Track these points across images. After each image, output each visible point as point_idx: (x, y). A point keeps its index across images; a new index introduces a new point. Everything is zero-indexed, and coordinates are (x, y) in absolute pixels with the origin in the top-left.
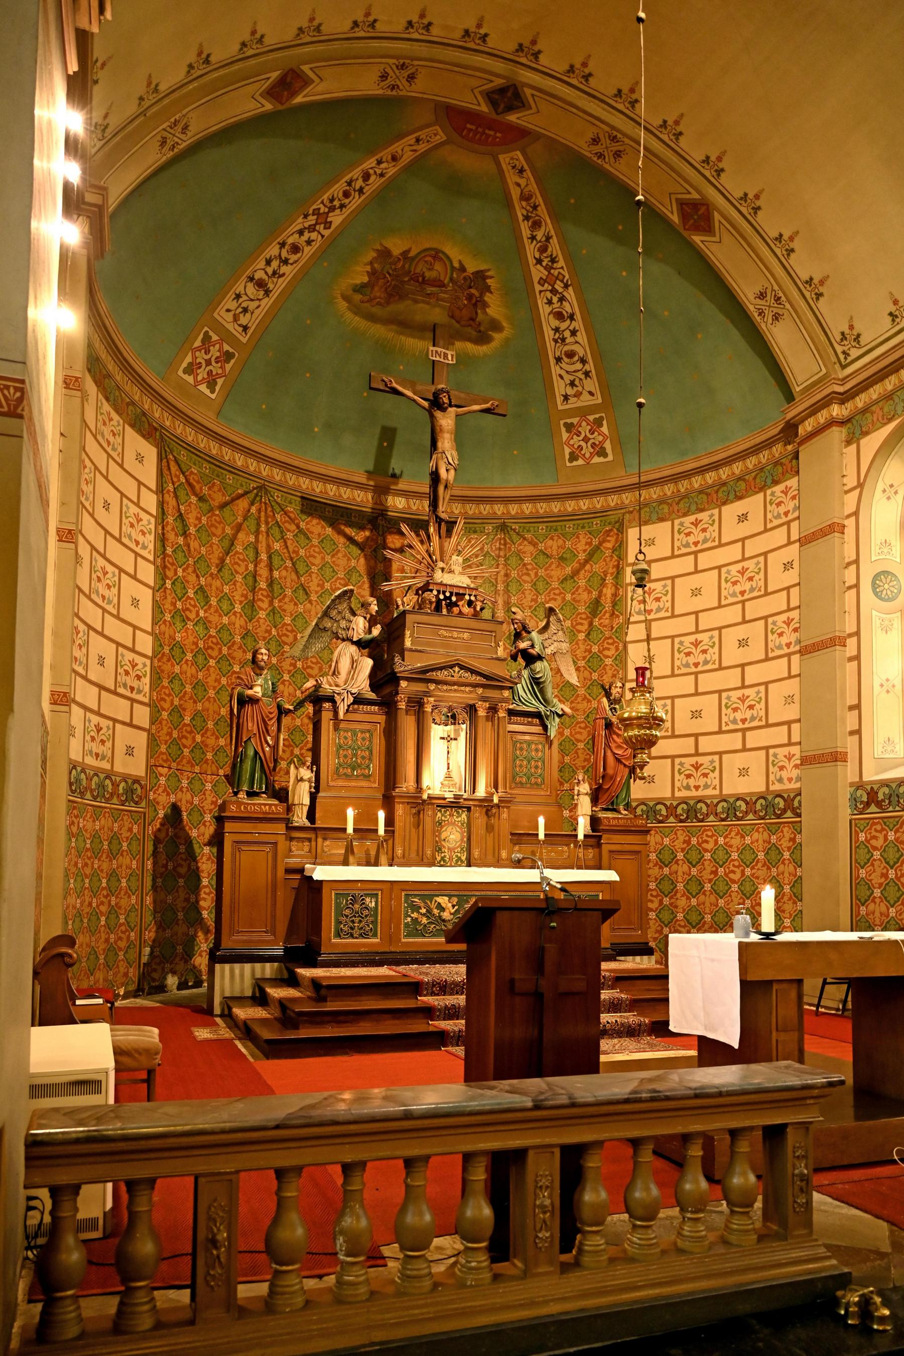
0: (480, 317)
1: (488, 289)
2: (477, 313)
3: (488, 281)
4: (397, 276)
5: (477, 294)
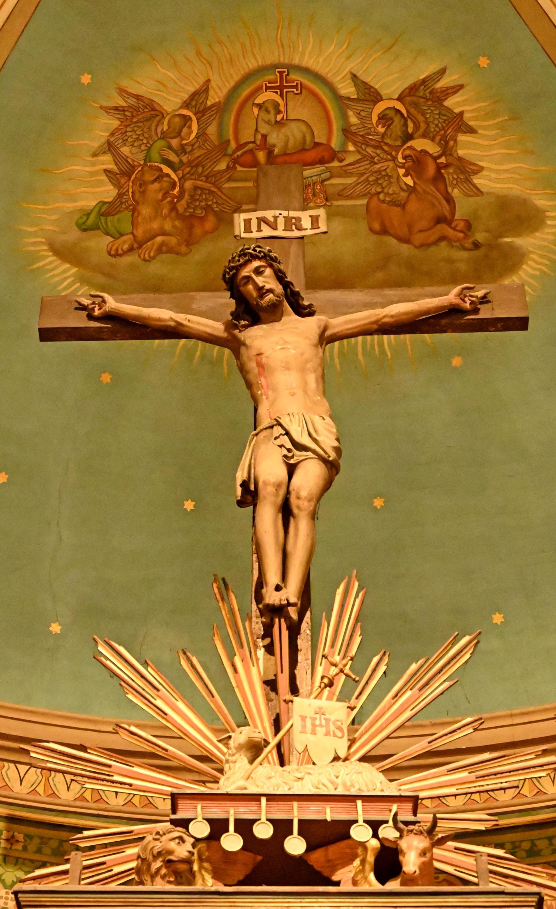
0: (464, 206)
1: (459, 123)
2: (449, 200)
3: (448, 103)
4: (194, 165)
5: (433, 148)
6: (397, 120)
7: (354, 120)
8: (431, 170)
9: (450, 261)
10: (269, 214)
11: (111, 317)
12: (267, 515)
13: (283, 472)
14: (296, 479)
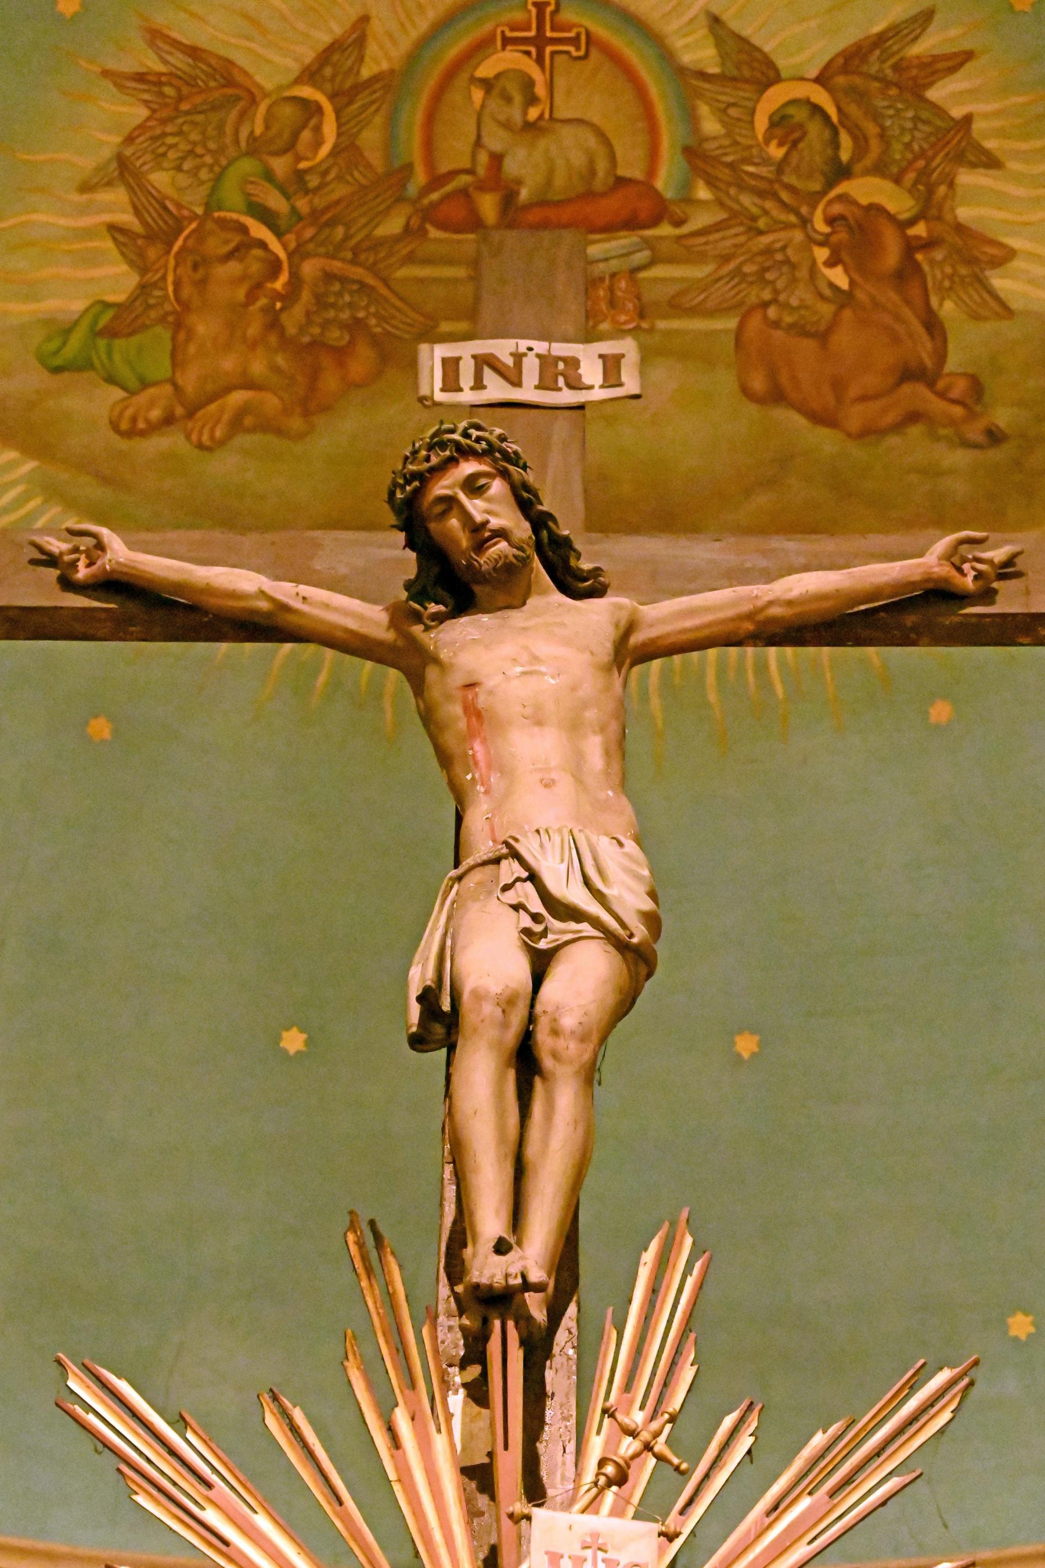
0: (967, 344)
2: (933, 325)
4: (323, 219)
5: (897, 201)
6: (815, 130)
7: (711, 126)
8: (892, 256)
9: (932, 472)
10: (503, 349)
11: (117, 585)
12: (481, 1072)
13: (520, 970)
14: (550, 989)
